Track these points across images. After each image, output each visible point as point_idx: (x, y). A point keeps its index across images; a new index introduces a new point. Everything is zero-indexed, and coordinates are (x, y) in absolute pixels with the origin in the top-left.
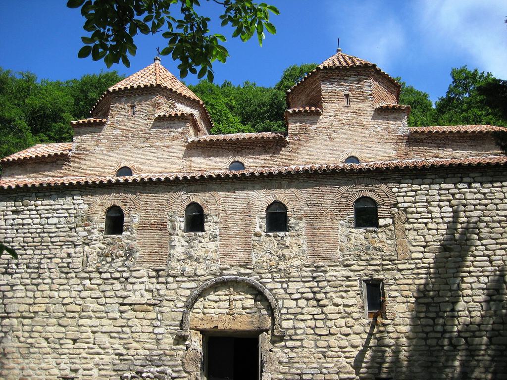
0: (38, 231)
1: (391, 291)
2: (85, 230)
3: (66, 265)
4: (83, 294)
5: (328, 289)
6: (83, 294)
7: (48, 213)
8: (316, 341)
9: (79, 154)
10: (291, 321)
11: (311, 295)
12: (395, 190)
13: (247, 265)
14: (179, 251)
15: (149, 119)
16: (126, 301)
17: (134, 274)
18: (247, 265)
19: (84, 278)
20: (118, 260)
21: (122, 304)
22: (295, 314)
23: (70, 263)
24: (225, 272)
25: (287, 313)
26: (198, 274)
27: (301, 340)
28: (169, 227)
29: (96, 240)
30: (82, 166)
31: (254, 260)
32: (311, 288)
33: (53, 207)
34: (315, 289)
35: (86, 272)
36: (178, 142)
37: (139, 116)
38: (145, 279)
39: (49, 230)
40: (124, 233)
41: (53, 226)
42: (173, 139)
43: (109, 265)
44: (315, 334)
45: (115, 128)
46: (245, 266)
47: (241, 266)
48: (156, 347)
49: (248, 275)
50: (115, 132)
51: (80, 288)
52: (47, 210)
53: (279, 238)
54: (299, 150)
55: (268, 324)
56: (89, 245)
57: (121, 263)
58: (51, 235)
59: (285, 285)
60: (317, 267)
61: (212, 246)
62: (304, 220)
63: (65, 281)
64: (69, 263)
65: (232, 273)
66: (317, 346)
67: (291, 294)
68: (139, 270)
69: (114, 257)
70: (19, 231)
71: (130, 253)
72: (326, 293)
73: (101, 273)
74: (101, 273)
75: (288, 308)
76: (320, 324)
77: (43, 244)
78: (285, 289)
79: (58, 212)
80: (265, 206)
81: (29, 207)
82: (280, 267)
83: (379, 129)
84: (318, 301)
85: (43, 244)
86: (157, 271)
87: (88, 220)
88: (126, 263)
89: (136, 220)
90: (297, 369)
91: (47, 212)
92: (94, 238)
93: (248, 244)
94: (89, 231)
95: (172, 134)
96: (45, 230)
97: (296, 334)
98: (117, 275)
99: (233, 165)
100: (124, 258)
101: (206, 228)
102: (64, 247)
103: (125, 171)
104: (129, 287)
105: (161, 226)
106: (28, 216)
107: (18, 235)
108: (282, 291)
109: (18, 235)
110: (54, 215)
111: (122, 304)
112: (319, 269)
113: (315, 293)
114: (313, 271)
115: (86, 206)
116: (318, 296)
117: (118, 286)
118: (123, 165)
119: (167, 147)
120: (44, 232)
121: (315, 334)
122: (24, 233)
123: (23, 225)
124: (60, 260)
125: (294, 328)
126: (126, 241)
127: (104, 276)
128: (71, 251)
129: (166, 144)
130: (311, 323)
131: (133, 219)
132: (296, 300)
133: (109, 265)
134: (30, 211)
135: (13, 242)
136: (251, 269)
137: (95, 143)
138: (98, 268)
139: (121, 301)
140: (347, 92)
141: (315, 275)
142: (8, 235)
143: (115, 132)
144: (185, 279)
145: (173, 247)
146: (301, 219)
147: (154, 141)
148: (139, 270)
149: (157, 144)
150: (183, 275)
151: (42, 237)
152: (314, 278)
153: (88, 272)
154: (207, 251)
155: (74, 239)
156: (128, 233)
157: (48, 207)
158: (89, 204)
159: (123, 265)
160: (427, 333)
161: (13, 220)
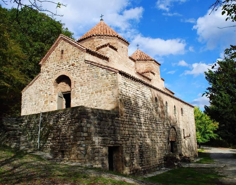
15: (127, 56)
119: (131, 70)
129: (131, 69)
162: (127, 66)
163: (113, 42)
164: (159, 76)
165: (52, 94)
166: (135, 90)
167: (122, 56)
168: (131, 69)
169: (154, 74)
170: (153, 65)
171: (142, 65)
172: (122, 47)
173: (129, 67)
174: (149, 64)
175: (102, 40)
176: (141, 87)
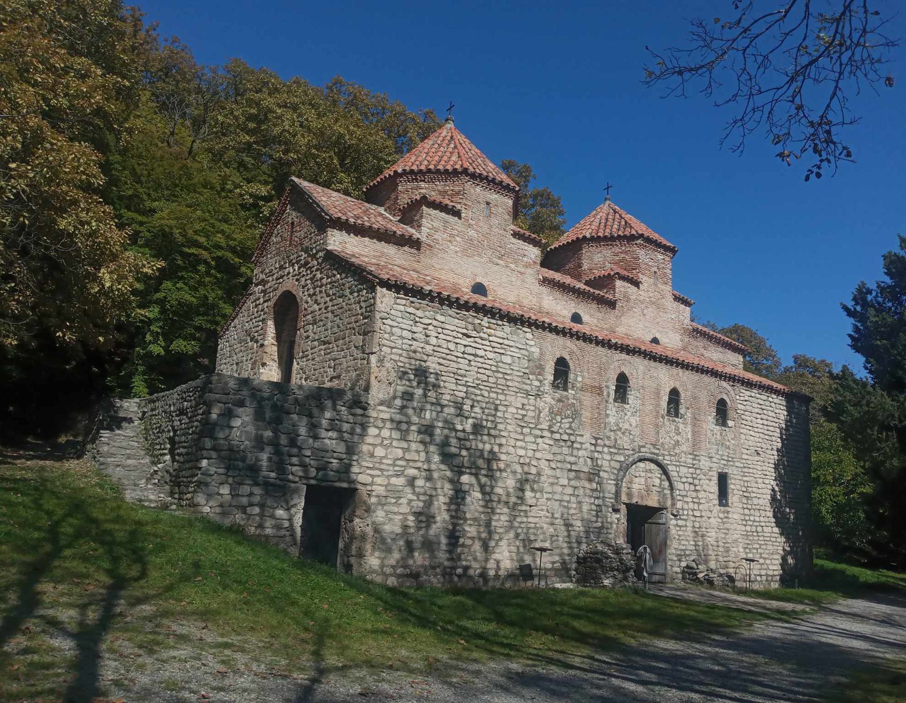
0: (494, 368)
1: (734, 486)
2: (537, 380)
3: (521, 417)
4: (538, 455)
5: (702, 476)
6: (538, 455)
7: (502, 348)
8: (694, 522)
9: (431, 246)
10: (681, 502)
11: (690, 480)
12: (738, 397)
13: (656, 445)
14: (612, 420)
15: (505, 230)
16: (574, 467)
17: (579, 439)
18: (656, 445)
19: (536, 437)
20: (566, 421)
21: (570, 470)
22: (683, 496)
23: (525, 415)
24: (643, 450)
25: (679, 495)
26: (625, 447)
27: (686, 520)
28: (605, 394)
29: (546, 393)
30: (434, 264)
31: (661, 441)
32: (692, 474)
33: (506, 342)
34: (695, 476)
35: (539, 429)
36: (529, 271)
37: (495, 221)
38: (587, 445)
39: (504, 371)
40: (570, 391)
41: (507, 367)
42: (527, 266)
43: (559, 424)
44: (694, 515)
45: (470, 226)
46: (654, 445)
47: (652, 444)
48: (594, 519)
49: (657, 455)
50: (472, 233)
51: (534, 447)
52: (501, 344)
53: (675, 423)
54: (623, 318)
55: (669, 503)
56: (541, 398)
57: (567, 426)
58: (506, 377)
59: (678, 469)
60: (696, 455)
61: (633, 420)
62: (690, 411)
63: (521, 437)
64: (524, 416)
65: (646, 452)
66: (694, 527)
67: (681, 477)
68: (582, 436)
69: (563, 417)
70: (472, 363)
71: (576, 415)
72: (700, 480)
73: (552, 432)
74: (552, 432)
75: (680, 490)
76: (696, 507)
77: (499, 386)
78: (678, 472)
79: (512, 349)
80: (668, 390)
81: (482, 335)
82: (676, 451)
83: (673, 317)
84: (695, 486)
85: (499, 386)
86: (596, 439)
87: (539, 369)
88: (573, 425)
89: (580, 379)
90: (684, 545)
91: (499, 346)
92: (546, 391)
93: (657, 426)
94: (541, 381)
95: (525, 259)
96: (501, 370)
97: (683, 515)
98: (566, 437)
99: (576, 318)
100: (571, 420)
101: (630, 402)
102: (519, 395)
103: (479, 289)
104: (575, 452)
105: (598, 390)
106: (480, 346)
107: (470, 368)
108: (676, 474)
109: (470, 368)
110: (507, 353)
111: (570, 470)
112: (697, 458)
113: (694, 478)
114: (694, 459)
115: (538, 350)
116: (696, 482)
117: (565, 450)
118: (478, 280)
119: (521, 273)
120: (498, 372)
121: (694, 515)
122: (479, 368)
123: (476, 355)
124: (515, 411)
125: (683, 509)
126: (573, 401)
127: (557, 436)
128: (525, 401)
129: (519, 269)
130: (691, 505)
131: (577, 377)
132: (684, 483)
133: (559, 424)
134: (482, 339)
135: (465, 376)
136: (658, 449)
137: (449, 239)
138: (550, 427)
139: (569, 466)
140: (655, 269)
141: (694, 462)
142: (461, 366)
143: (472, 233)
144: (616, 451)
145: (607, 415)
146: (688, 408)
147: (509, 260)
148: (582, 436)
149: (513, 266)
150: (614, 447)
151: (497, 378)
152: (694, 465)
153: (541, 430)
154: (631, 425)
155: (528, 388)
156: (573, 392)
157: (501, 341)
158: (541, 349)
159: (570, 428)
160: (746, 521)
161: (465, 346)
162: (501, 262)
163: (452, 190)
164: (668, 288)
165: (266, 343)
166: (454, 334)
167: (485, 228)
168: (523, 270)
169: (636, 284)
170: (641, 253)
171: (599, 255)
172: (488, 203)
173: (513, 266)
174: (623, 248)
175: (422, 184)
176: (487, 325)
